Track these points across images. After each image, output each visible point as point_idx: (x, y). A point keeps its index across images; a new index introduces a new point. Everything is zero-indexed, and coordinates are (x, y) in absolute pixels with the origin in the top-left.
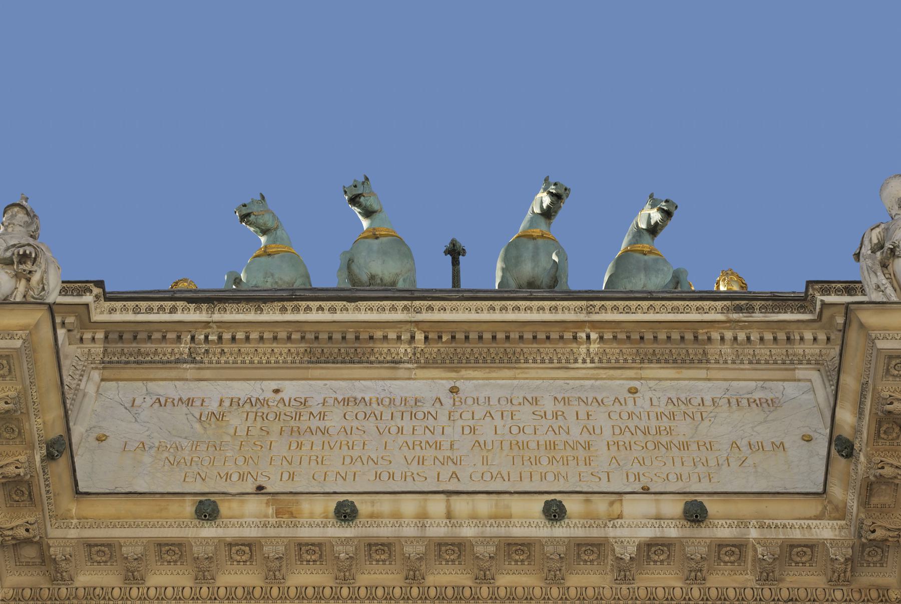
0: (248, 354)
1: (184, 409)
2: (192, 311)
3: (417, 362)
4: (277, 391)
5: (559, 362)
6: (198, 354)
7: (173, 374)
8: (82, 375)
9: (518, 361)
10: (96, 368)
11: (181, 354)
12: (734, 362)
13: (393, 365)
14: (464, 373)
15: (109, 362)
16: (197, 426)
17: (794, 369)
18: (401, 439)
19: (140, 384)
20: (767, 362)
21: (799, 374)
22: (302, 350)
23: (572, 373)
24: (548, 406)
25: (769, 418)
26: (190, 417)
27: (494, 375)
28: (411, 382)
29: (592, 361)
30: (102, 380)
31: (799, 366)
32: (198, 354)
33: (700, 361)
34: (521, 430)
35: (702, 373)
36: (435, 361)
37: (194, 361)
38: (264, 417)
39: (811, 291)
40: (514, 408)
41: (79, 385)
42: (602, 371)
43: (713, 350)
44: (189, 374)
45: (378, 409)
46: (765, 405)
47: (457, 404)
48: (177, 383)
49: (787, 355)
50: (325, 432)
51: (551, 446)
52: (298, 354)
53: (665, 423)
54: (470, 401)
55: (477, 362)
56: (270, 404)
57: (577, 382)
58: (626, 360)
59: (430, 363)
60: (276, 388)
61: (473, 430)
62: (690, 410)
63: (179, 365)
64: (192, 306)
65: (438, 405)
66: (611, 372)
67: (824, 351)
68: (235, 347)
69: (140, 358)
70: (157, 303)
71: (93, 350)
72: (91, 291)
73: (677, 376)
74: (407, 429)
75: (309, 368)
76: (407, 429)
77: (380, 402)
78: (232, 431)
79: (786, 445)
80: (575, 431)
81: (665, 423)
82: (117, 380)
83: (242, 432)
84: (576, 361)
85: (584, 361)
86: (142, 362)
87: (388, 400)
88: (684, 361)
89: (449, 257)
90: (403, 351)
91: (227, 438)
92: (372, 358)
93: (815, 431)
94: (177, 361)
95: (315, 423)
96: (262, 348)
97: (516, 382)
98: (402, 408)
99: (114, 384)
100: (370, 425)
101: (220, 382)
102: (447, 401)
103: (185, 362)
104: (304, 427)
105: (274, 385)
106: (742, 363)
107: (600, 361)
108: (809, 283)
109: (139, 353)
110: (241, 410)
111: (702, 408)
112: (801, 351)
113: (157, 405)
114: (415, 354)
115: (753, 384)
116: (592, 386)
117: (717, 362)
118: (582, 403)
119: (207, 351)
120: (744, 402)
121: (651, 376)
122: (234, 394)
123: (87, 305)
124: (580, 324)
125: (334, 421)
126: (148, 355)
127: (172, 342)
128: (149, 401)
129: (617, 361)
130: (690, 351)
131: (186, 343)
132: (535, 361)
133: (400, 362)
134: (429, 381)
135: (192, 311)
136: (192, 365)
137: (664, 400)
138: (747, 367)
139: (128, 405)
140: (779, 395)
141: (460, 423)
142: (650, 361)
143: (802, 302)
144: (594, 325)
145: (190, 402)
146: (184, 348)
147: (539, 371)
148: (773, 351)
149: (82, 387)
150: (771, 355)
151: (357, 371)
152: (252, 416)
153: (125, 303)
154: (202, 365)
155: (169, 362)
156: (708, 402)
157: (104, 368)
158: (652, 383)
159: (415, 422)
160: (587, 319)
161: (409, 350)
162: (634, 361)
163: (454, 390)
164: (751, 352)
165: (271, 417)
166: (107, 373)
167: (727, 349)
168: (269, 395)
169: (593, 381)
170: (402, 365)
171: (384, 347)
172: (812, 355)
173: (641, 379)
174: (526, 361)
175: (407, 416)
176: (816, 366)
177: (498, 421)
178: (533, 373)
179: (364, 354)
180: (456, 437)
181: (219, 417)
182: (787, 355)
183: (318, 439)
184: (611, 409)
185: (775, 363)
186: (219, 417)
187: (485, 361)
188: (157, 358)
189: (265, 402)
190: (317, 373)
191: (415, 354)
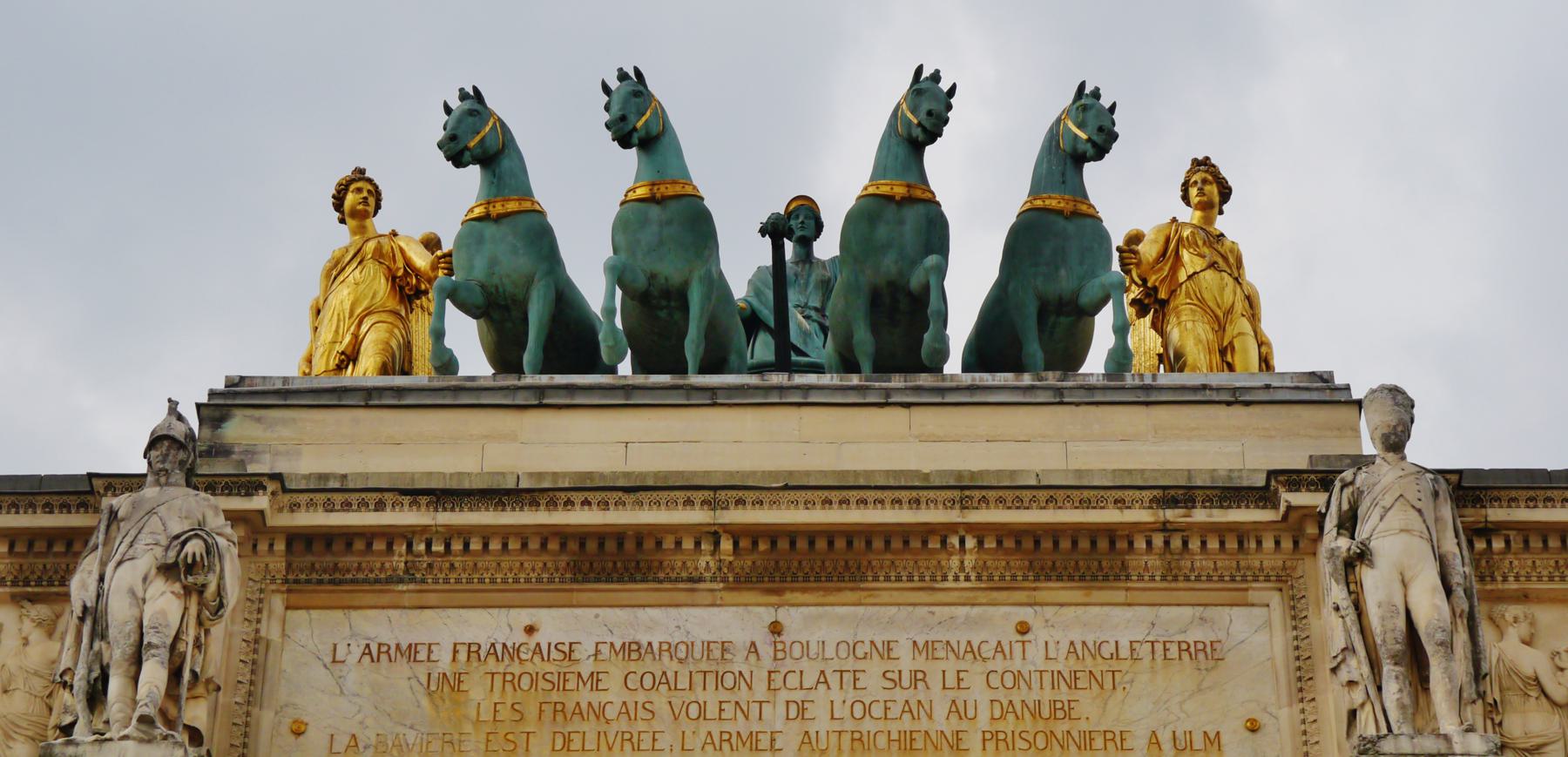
0: (487, 569)
1: (402, 668)
2: (406, 507)
3: (725, 580)
4: (530, 630)
5: (922, 579)
6: (418, 570)
7: (385, 599)
8: (260, 611)
9: (863, 579)
10: (278, 591)
11: (394, 570)
12: (1164, 578)
13: (689, 586)
14: (788, 596)
15: (296, 582)
16: (425, 702)
17: (1246, 590)
18: (704, 728)
19: (339, 614)
20: (1209, 579)
21: (1252, 596)
22: (563, 564)
23: (940, 597)
24: (906, 661)
25: (1205, 684)
26: (414, 682)
27: (831, 599)
28: (716, 610)
29: (967, 579)
30: (287, 608)
31: (1254, 585)
32: (418, 570)
33: (1117, 578)
34: (867, 710)
35: (1120, 596)
36: (748, 580)
37: (413, 580)
38: (513, 682)
39: (1273, 483)
40: (860, 665)
41: (257, 631)
42: (979, 593)
43: (1134, 562)
44: (406, 600)
45: (671, 666)
46: (1201, 656)
47: (780, 655)
48: (391, 612)
49: (1238, 569)
50: (599, 713)
52: (557, 570)
53: (1064, 694)
54: (797, 651)
55: (806, 579)
56: (523, 656)
57: (946, 609)
58: (1014, 578)
59: (741, 581)
60: (528, 622)
61: (802, 710)
62: (1099, 667)
63: (392, 587)
64: (407, 500)
65: (753, 657)
66: (995, 594)
67: (1289, 564)
68: (470, 560)
69: (338, 576)
70: (357, 495)
71: (271, 566)
72: (264, 488)
73: (1087, 600)
74: (712, 711)
75: (572, 590)
76: (712, 711)
77: (671, 649)
78: (473, 714)
79: (1224, 739)
80: (941, 711)
81: (1064, 694)
82: (308, 608)
83: (486, 716)
84: (945, 578)
85: (956, 579)
86: (341, 582)
87: (683, 647)
88: (1094, 578)
89: (768, 239)
90: (703, 564)
91: (468, 728)
92: (661, 575)
93: (1265, 710)
94: (389, 581)
95: (585, 696)
96: (506, 562)
97: (861, 610)
98: (704, 666)
99: (302, 613)
100: (660, 700)
101: (451, 612)
102: (766, 650)
103: (401, 581)
104: (570, 706)
105: (524, 617)
106: (1175, 579)
107: (979, 578)
108: (1271, 474)
109: (336, 568)
110: (483, 669)
111: (1115, 665)
112: (1257, 564)
113: (367, 658)
114: (720, 569)
115: (1188, 611)
116: (967, 617)
117: (1141, 578)
118: (951, 655)
119: (430, 566)
120: (1174, 649)
121: (1049, 600)
123: (262, 512)
124: (952, 528)
125: (613, 694)
126: (348, 571)
127: (380, 553)
128: (357, 651)
129: (1002, 578)
130: (1104, 564)
131: (400, 555)
132: (888, 579)
133: (700, 580)
134: (741, 610)
135: (406, 507)
136: (412, 587)
137: (1064, 647)
138: (1181, 585)
139: (328, 660)
140: (1221, 635)
141: (784, 695)
142: (1049, 579)
143: (1263, 496)
144: (971, 528)
145: (411, 652)
146: (398, 560)
147: (895, 593)
148: (1219, 564)
149: (263, 633)
150: (1216, 569)
151: (639, 591)
152: (498, 679)
153: (312, 496)
154: (425, 587)
155: (377, 581)
156: (1125, 653)
157: (289, 591)
158: (1050, 611)
159: (724, 696)
160: (959, 520)
161: (712, 564)
162: (1025, 578)
163: (776, 629)
164: (1189, 564)
165: (525, 681)
166: (294, 598)
167: (1154, 561)
168: (521, 637)
169: (967, 609)
170: (701, 586)
171: (678, 560)
172: (1273, 569)
173: (1036, 604)
174: (876, 579)
175: (711, 679)
176: (1279, 585)
177: (836, 694)
178: (885, 597)
179: (649, 569)
180: (778, 727)
181: (453, 684)
182: (1238, 569)
183: (590, 727)
184: (991, 666)
185: (1221, 579)
186: (453, 684)
187: (818, 580)
188: (361, 576)
189: (514, 653)
190: (585, 597)
191: (720, 569)
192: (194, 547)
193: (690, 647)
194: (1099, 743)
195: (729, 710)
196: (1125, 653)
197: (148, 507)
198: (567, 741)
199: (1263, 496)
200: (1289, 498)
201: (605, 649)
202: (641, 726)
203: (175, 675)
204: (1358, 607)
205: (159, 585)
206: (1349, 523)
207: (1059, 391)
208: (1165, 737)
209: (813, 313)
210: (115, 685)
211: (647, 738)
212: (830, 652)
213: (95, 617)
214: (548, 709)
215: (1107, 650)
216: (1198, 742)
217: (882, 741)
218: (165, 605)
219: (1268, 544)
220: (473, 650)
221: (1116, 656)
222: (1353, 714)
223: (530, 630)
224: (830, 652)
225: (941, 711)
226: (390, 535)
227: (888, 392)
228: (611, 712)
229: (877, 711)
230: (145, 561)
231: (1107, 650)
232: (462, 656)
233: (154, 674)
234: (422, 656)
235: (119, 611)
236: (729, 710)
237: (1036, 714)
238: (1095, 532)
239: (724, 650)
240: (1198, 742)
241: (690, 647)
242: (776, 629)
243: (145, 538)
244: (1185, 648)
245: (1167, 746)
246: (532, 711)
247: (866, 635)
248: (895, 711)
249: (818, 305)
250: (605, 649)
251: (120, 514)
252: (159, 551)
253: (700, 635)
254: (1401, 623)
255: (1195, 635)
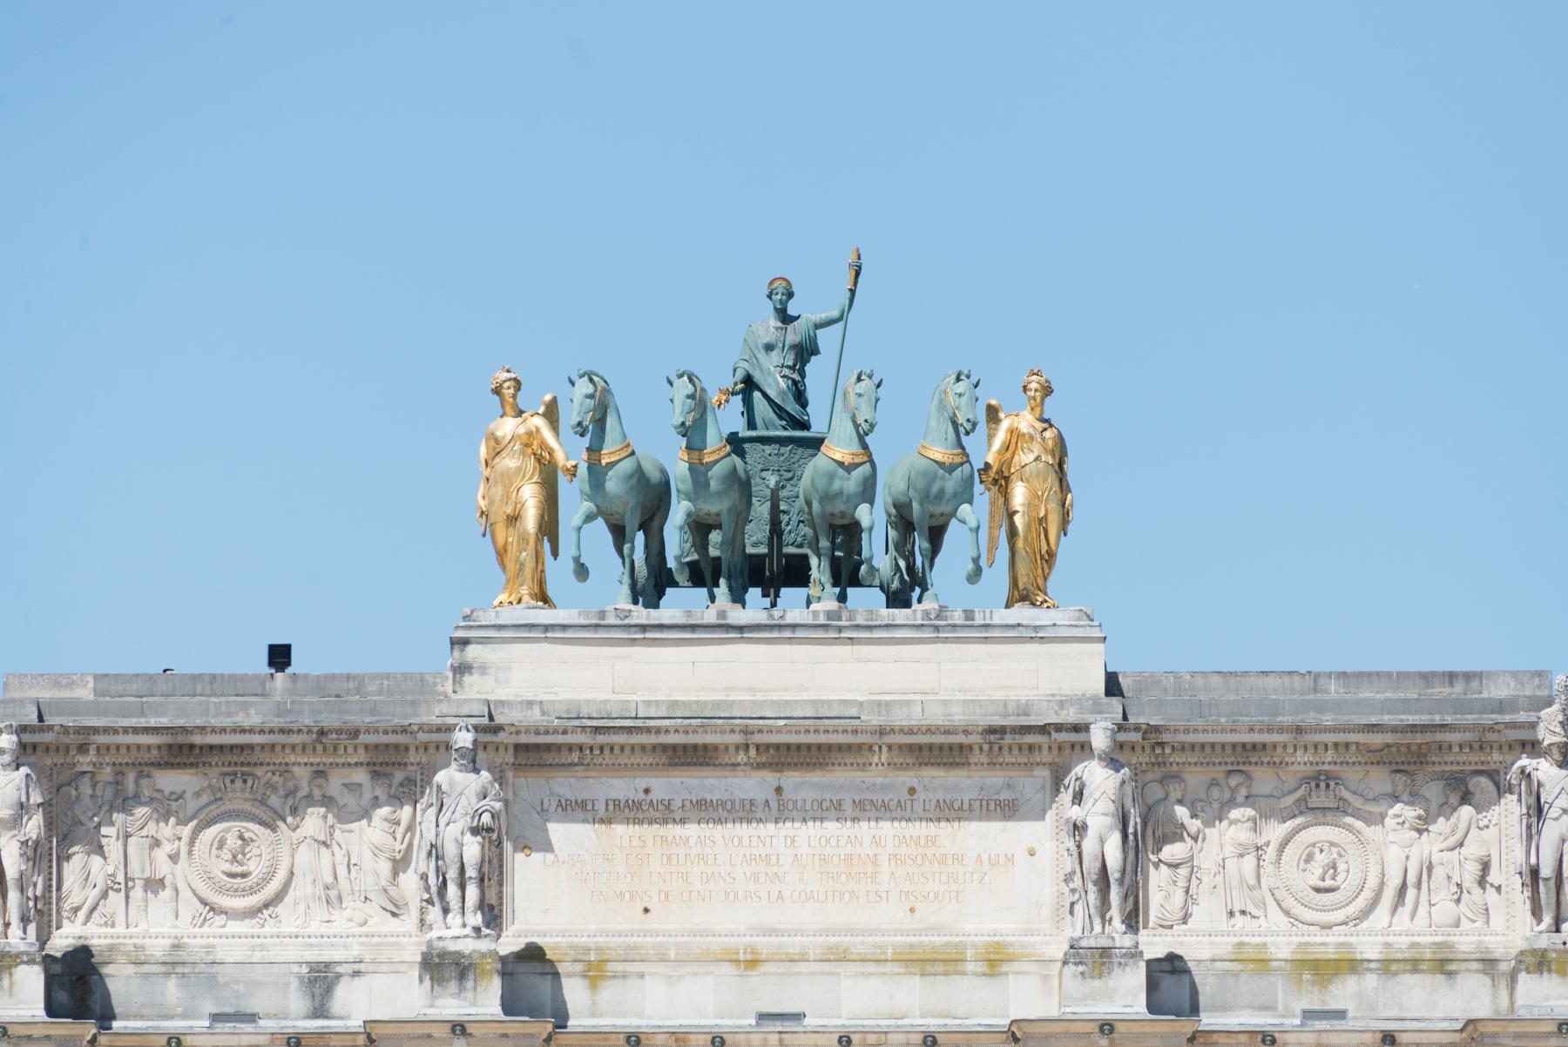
4: (647, 791)
34: (828, 841)
51: (849, 858)
59: (760, 766)
61: (793, 841)
74: (745, 841)
77: (723, 804)
80: (867, 842)
102: (774, 805)
105: (642, 783)
122: (615, 795)
128: (554, 804)
137: (934, 803)
146: (575, 757)
156: (966, 807)
163: (779, 790)
168: (641, 796)
192: (486, 819)
193: (733, 802)
194: (950, 861)
195: (754, 839)
196: (966, 807)
197: (459, 790)
198: (669, 857)
199: (1044, 729)
200: (1054, 735)
201: (687, 803)
202: (709, 851)
203: (482, 880)
204: (1079, 846)
205: (468, 837)
206: (1078, 797)
207: (937, 628)
208: (985, 857)
209: (787, 372)
210: (452, 890)
211: (711, 857)
212: (808, 807)
213: (435, 852)
214: (658, 839)
215: (957, 805)
216: (1002, 859)
217: (836, 860)
218: (473, 849)
219: (1045, 752)
220: (617, 803)
221: (961, 808)
222: (1073, 904)
223: (647, 791)
224: (808, 807)
225: (867, 842)
226: (570, 748)
227: (840, 629)
228: (692, 842)
229: (833, 842)
230: (463, 822)
231: (957, 805)
232: (611, 807)
233: (472, 892)
234: (589, 807)
235: (450, 850)
236: (754, 839)
237: (917, 844)
238: (951, 747)
239: (752, 805)
240: (1002, 859)
241: (733, 802)
242: (779, 790)
243: (460, 810)
244: (998, 803)
245: (986, 862)
246: (650, 841)
247: (828, 796)
248: (843, 842)
249: (790, 363)
250: (687, 803)
251: (444, 788)
252: (468, 818)
253: (739, 795)
254: (1098, 864)
255: (1004, 795)
